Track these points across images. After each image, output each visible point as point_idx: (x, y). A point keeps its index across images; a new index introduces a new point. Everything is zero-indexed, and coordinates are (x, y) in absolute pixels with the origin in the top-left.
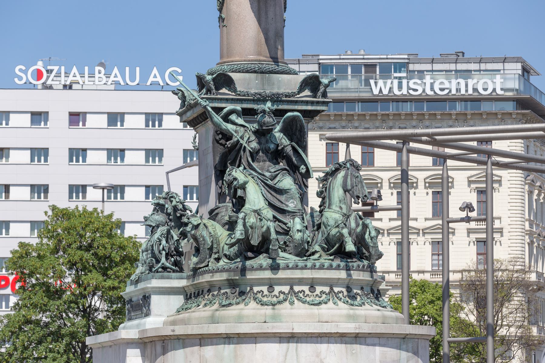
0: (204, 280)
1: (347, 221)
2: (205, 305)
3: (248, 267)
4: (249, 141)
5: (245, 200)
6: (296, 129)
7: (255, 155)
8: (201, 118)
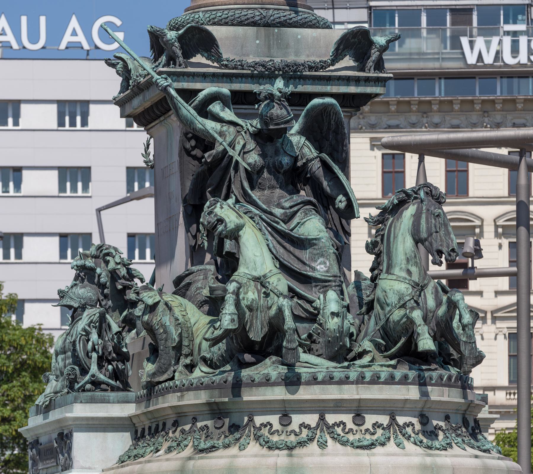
0: (166, 405)
1: (420, 295)
2: (169, 450)
3: (244, 379)
4: (244, 152)
5: (238, 260)
6: (329, 129)
7: (255, 177)
8: (158, 109)
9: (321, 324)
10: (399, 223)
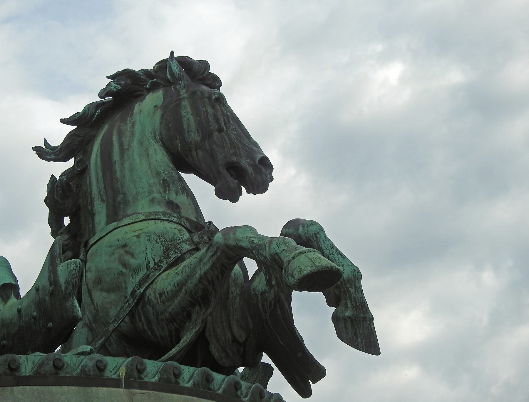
10: (129, 125)
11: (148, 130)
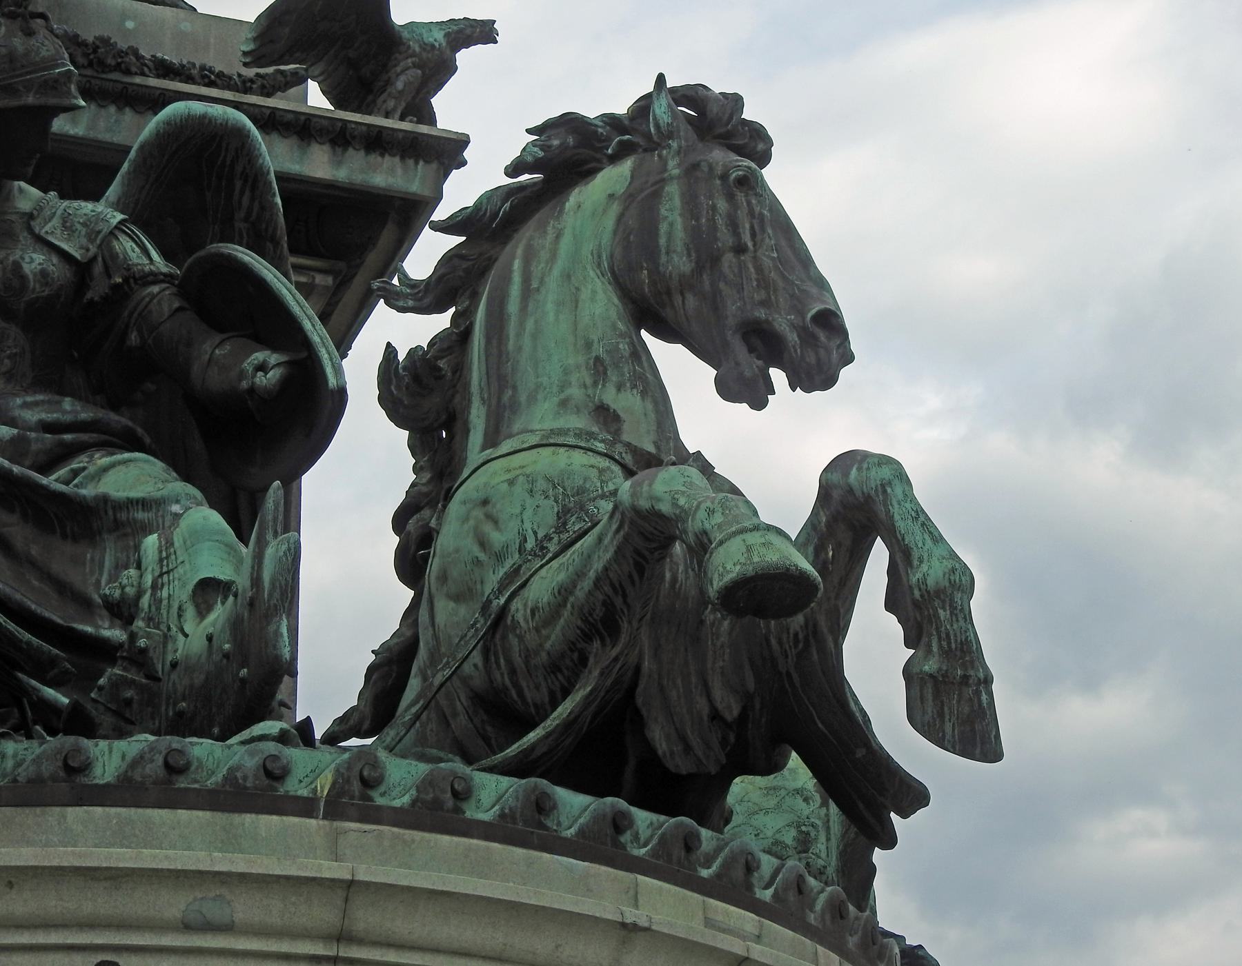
9: (143, 651)
10: (550, 237)
11: (587, 249)
